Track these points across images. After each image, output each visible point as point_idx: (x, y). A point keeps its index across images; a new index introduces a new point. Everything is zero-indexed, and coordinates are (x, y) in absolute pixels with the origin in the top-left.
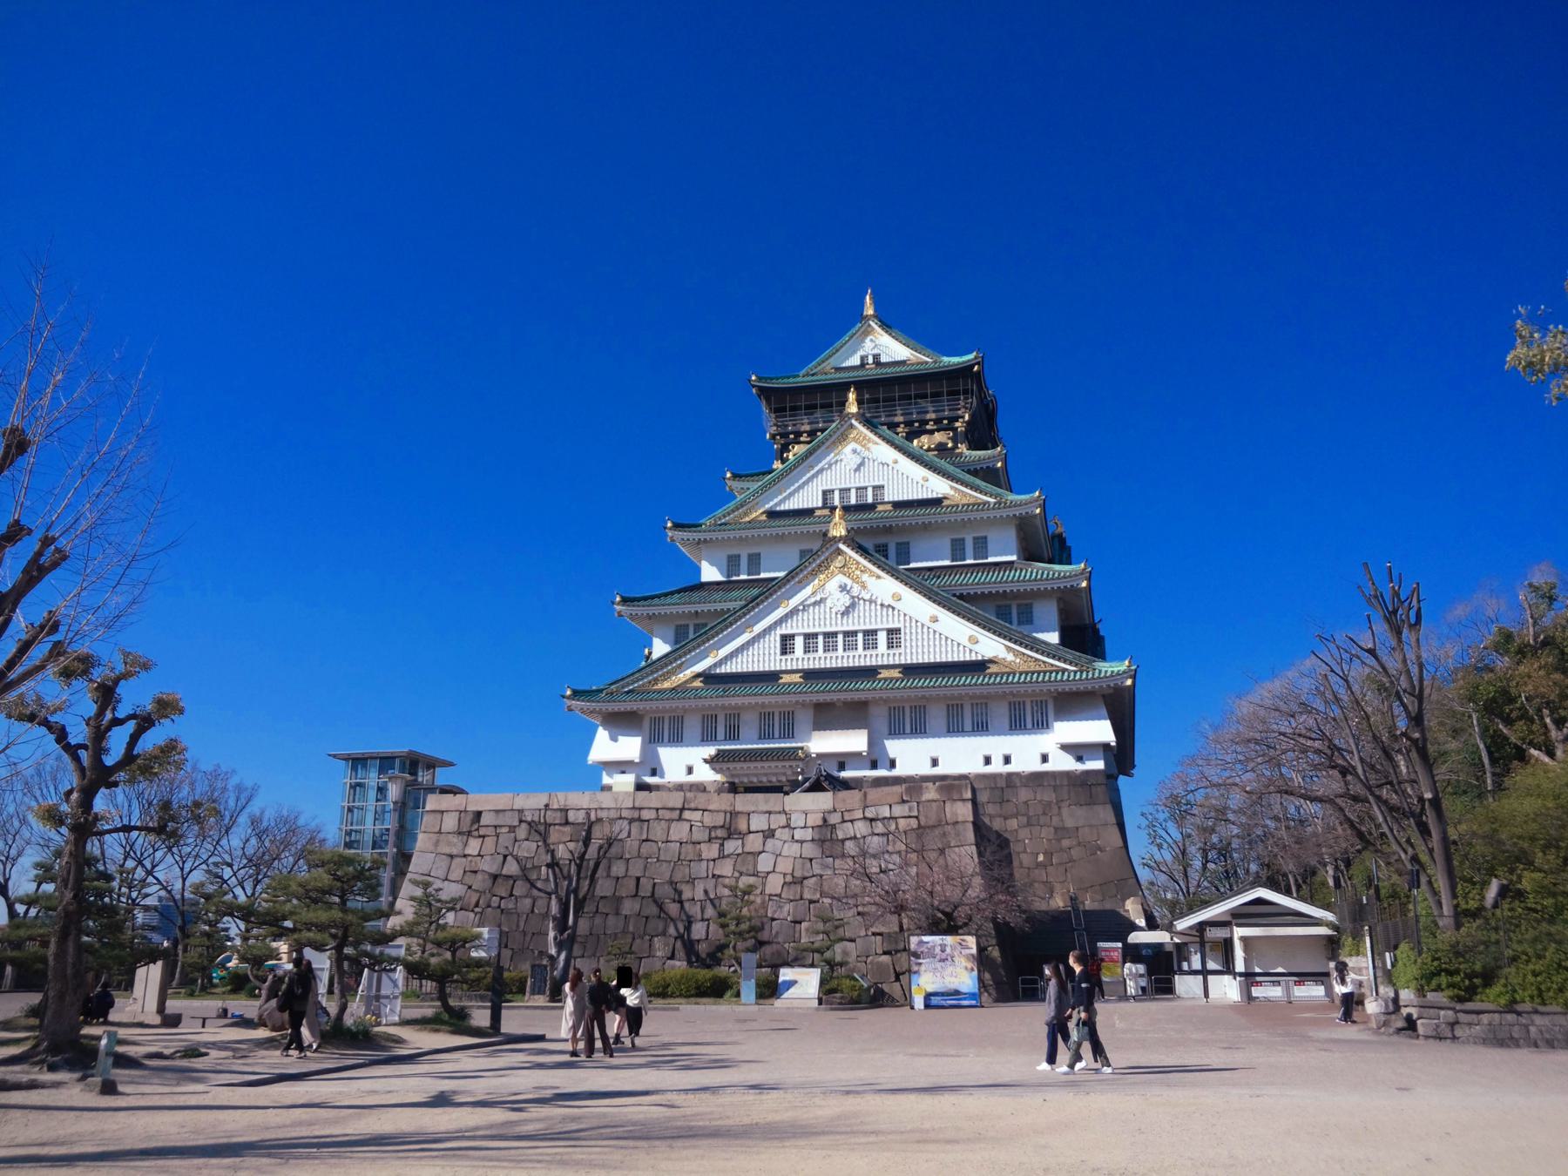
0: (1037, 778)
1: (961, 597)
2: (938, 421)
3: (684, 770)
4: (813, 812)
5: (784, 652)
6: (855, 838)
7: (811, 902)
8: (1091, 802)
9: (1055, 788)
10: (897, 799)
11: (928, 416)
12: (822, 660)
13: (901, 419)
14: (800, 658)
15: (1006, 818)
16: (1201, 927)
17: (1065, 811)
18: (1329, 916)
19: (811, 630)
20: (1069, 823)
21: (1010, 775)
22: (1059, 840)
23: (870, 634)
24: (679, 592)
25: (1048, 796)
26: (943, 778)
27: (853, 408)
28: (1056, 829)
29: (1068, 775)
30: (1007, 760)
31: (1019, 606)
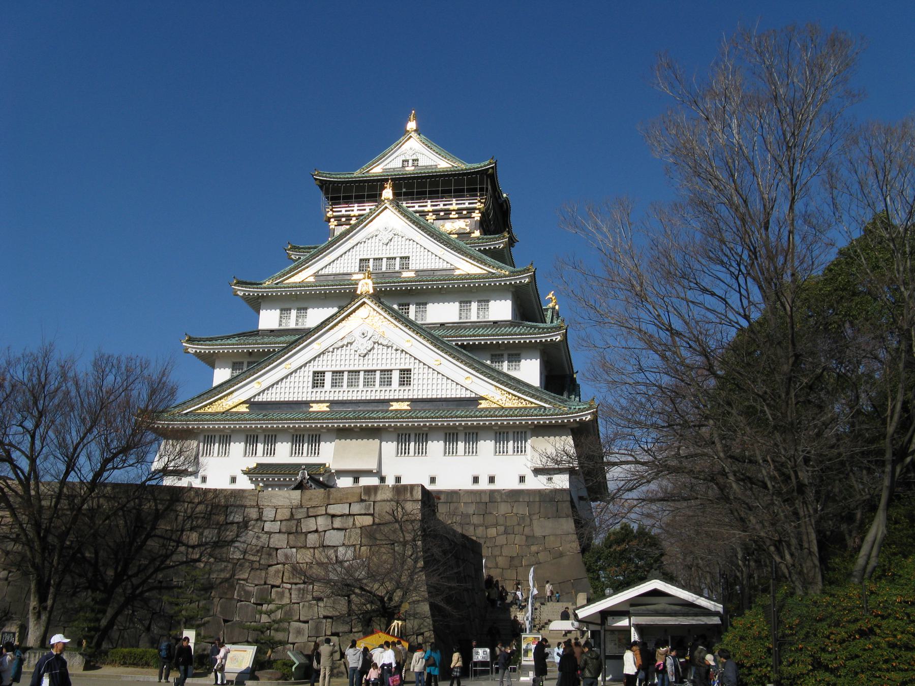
0: (514, 495)
1: (462, 346)
2: (459, 211)
3: (228, 480)
4: (282, 507)
5: (315, 385)
6: (316, 531)
7: (273, 586)
8: (557, 515)
9: (528, 504)
10: (355, 499)
11: (451, 207)
12: (345, 393)
13: (429, 208)
14: (329, 392)
15: (487, 528)
16: (605, 614)
17: (535, 523)
18: (719, 608)
19: (338, 368)
20: (538, 532)
21: (492, 492)
22: (528, 546)
23: (387, 372)
24: (239, 335)
25: (523, 510)
26: (440, 492)
27: (388, 193)
28: (527, 537)
29: (539, 492)
30: (492, 480)
31: (509, 355)
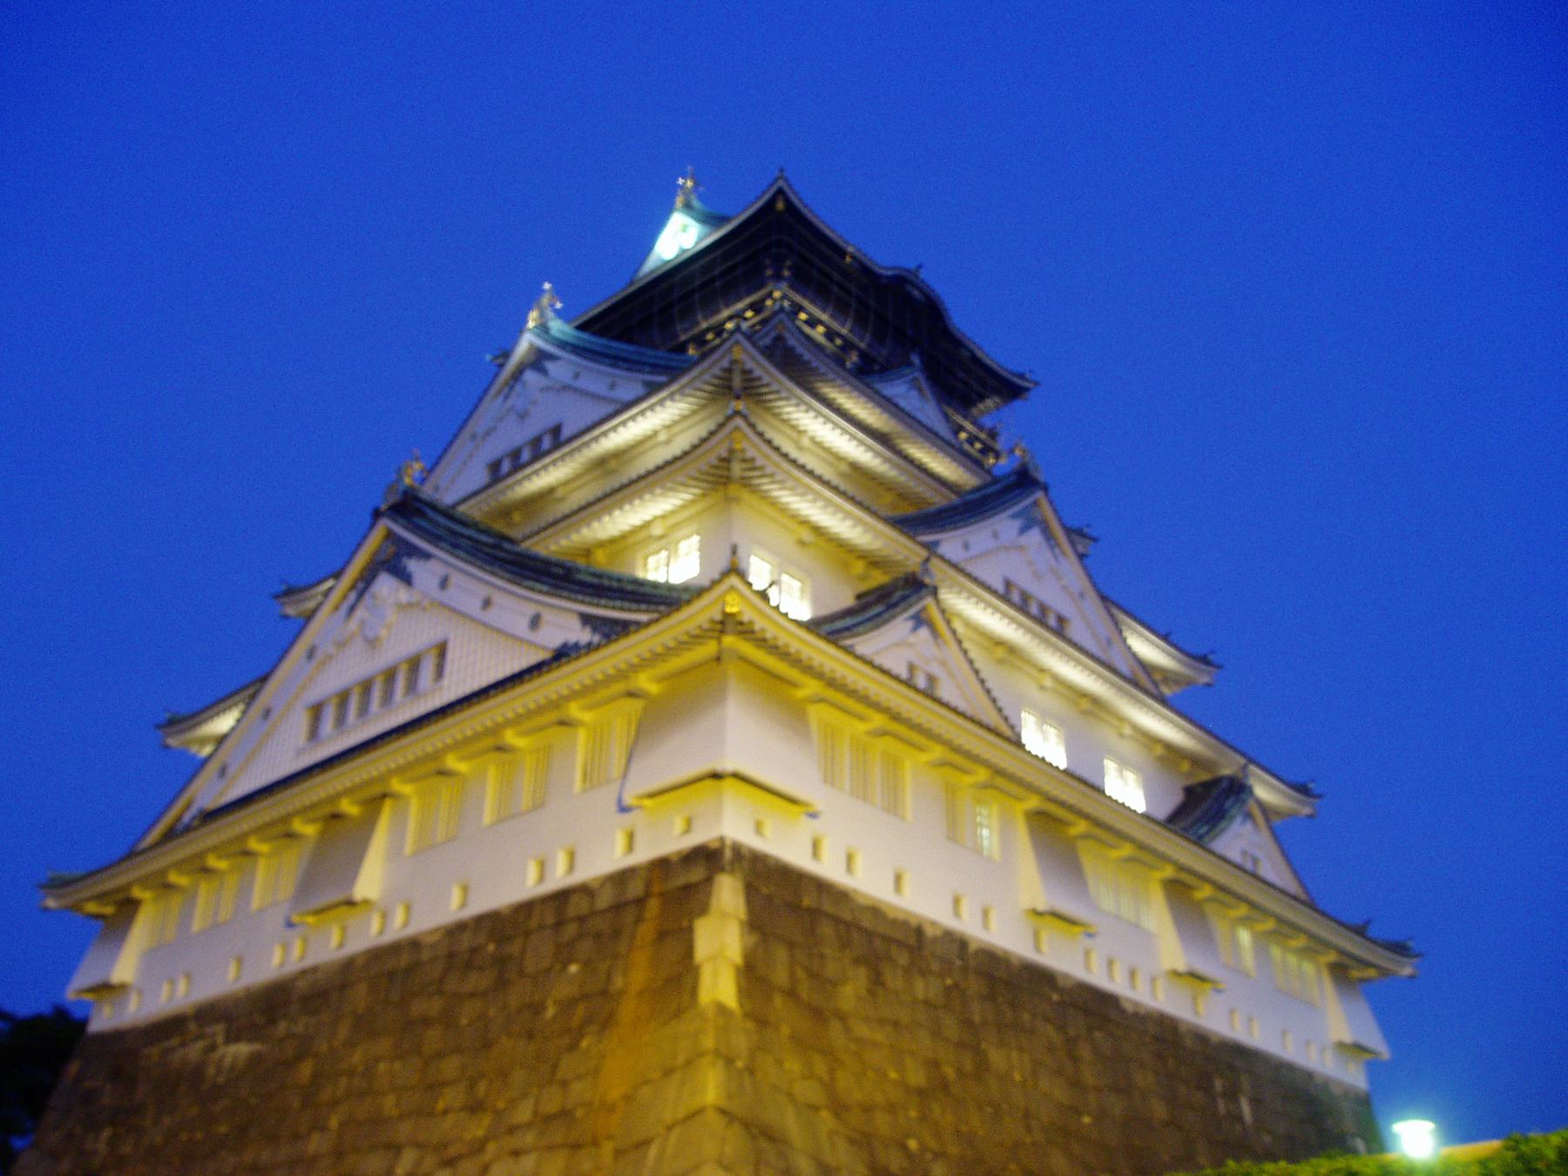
21: (562, 897)
23: (414, 664)
